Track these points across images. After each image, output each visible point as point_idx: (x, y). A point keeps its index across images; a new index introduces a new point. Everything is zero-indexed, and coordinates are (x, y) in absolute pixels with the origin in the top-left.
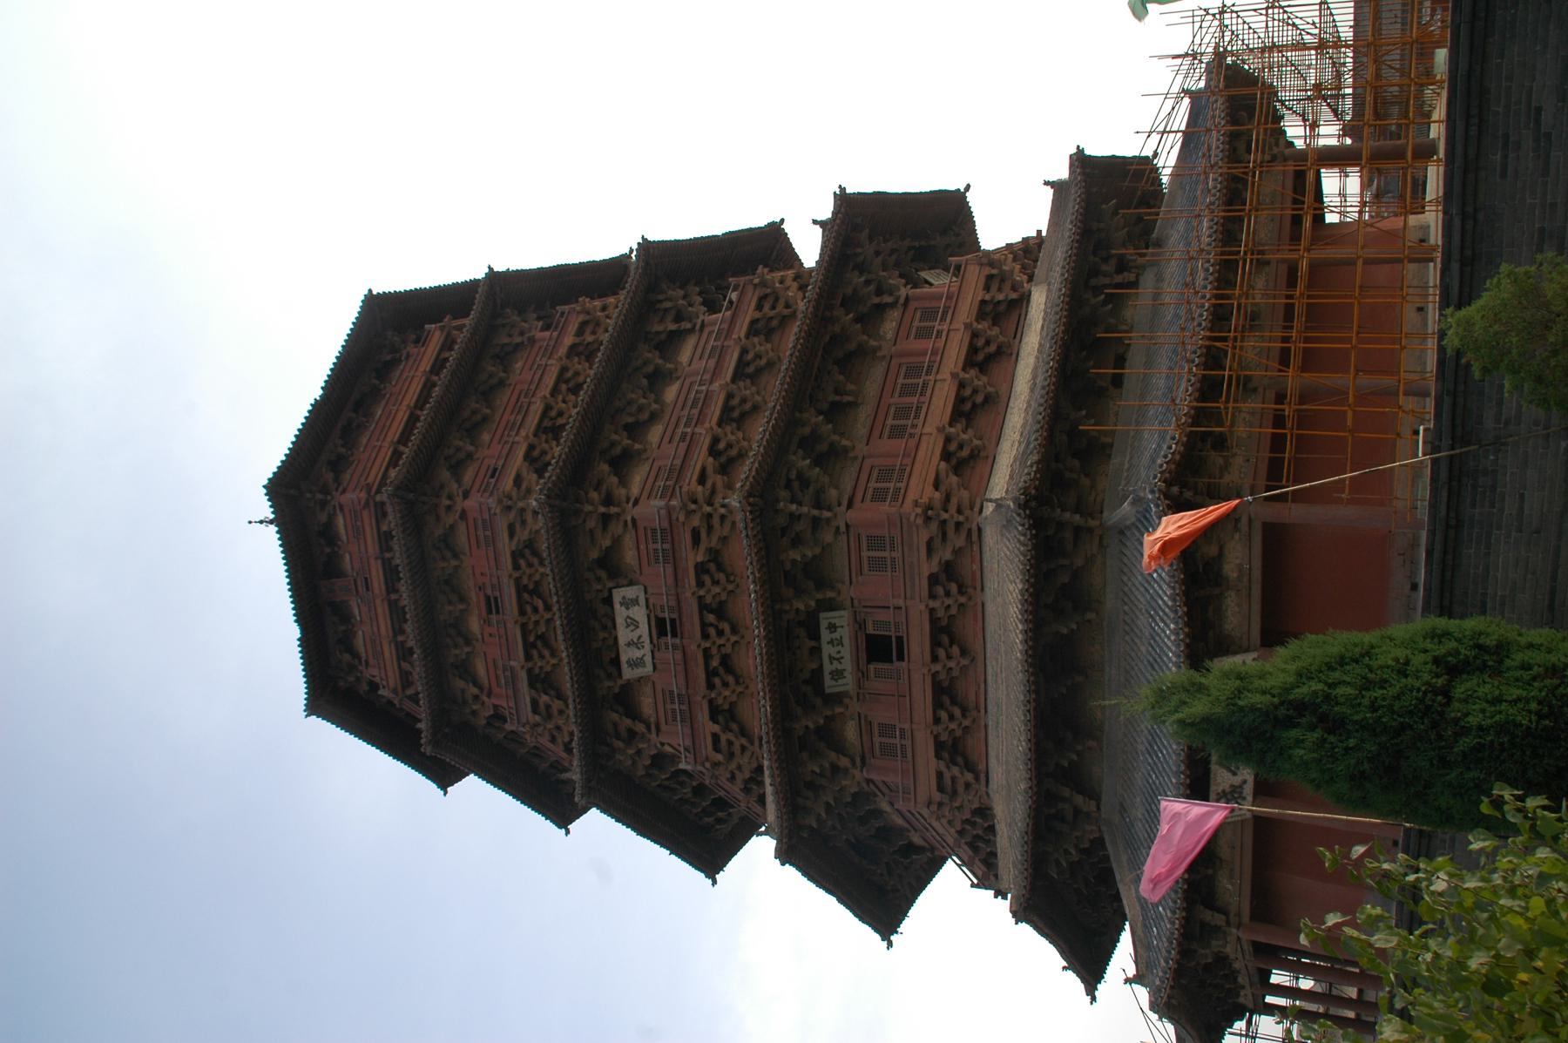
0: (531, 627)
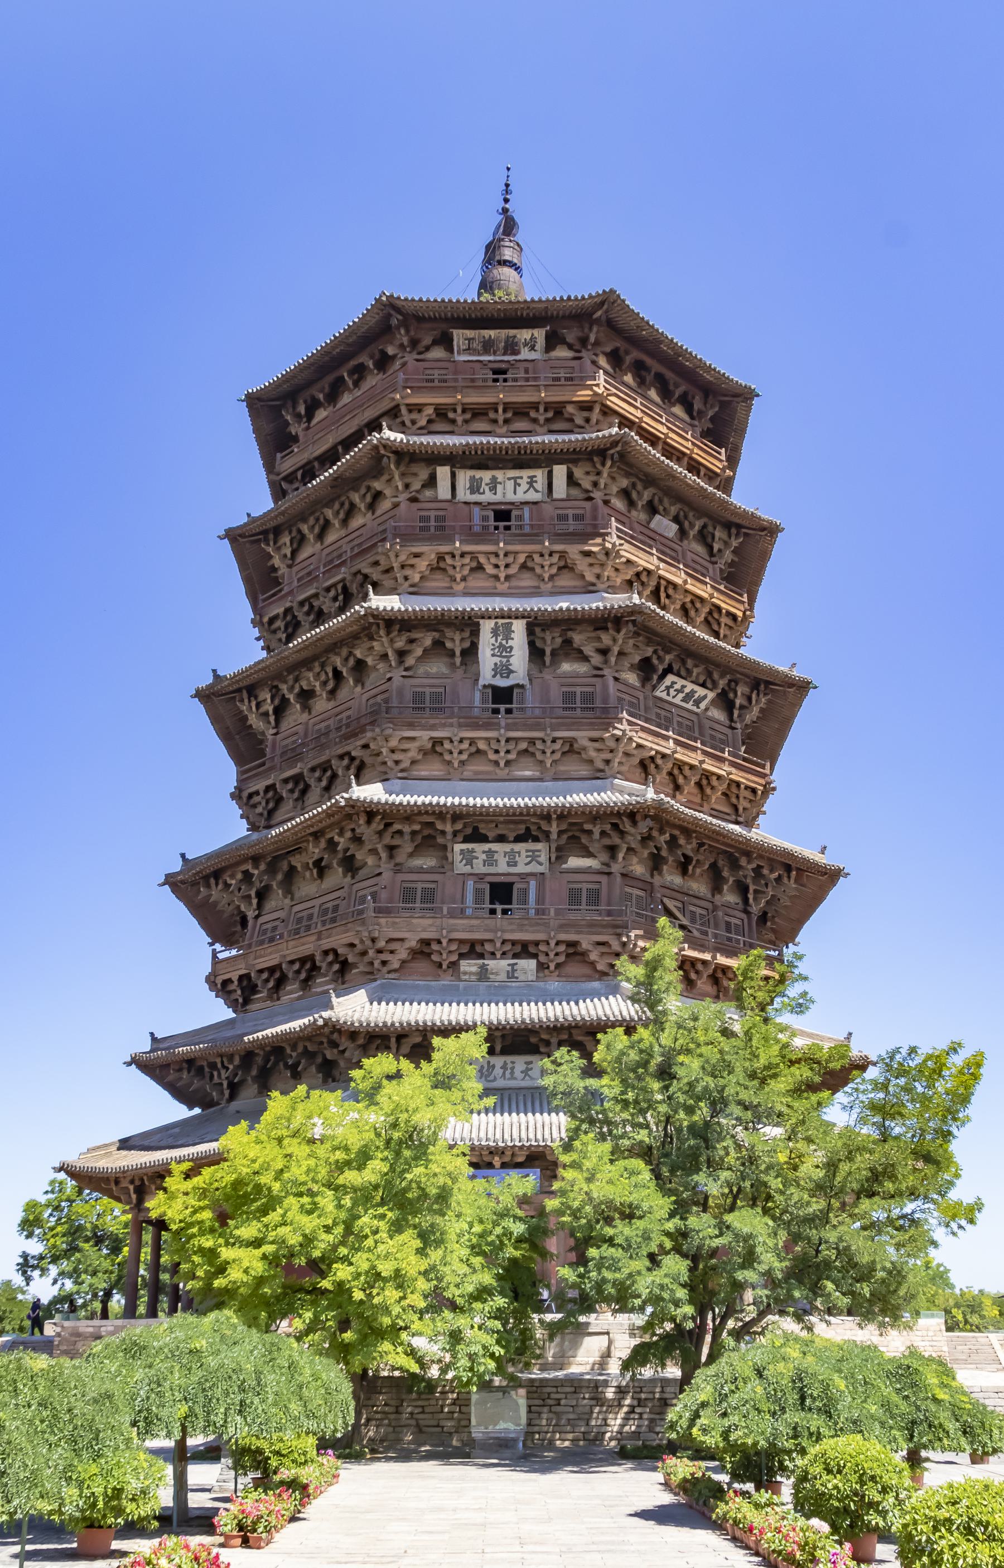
0: (493, 560)
